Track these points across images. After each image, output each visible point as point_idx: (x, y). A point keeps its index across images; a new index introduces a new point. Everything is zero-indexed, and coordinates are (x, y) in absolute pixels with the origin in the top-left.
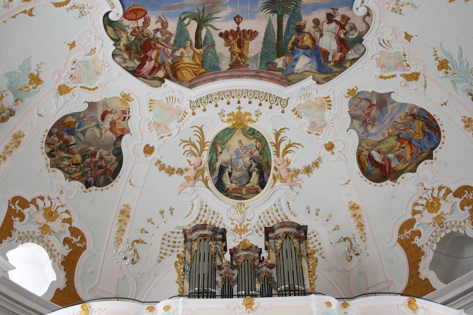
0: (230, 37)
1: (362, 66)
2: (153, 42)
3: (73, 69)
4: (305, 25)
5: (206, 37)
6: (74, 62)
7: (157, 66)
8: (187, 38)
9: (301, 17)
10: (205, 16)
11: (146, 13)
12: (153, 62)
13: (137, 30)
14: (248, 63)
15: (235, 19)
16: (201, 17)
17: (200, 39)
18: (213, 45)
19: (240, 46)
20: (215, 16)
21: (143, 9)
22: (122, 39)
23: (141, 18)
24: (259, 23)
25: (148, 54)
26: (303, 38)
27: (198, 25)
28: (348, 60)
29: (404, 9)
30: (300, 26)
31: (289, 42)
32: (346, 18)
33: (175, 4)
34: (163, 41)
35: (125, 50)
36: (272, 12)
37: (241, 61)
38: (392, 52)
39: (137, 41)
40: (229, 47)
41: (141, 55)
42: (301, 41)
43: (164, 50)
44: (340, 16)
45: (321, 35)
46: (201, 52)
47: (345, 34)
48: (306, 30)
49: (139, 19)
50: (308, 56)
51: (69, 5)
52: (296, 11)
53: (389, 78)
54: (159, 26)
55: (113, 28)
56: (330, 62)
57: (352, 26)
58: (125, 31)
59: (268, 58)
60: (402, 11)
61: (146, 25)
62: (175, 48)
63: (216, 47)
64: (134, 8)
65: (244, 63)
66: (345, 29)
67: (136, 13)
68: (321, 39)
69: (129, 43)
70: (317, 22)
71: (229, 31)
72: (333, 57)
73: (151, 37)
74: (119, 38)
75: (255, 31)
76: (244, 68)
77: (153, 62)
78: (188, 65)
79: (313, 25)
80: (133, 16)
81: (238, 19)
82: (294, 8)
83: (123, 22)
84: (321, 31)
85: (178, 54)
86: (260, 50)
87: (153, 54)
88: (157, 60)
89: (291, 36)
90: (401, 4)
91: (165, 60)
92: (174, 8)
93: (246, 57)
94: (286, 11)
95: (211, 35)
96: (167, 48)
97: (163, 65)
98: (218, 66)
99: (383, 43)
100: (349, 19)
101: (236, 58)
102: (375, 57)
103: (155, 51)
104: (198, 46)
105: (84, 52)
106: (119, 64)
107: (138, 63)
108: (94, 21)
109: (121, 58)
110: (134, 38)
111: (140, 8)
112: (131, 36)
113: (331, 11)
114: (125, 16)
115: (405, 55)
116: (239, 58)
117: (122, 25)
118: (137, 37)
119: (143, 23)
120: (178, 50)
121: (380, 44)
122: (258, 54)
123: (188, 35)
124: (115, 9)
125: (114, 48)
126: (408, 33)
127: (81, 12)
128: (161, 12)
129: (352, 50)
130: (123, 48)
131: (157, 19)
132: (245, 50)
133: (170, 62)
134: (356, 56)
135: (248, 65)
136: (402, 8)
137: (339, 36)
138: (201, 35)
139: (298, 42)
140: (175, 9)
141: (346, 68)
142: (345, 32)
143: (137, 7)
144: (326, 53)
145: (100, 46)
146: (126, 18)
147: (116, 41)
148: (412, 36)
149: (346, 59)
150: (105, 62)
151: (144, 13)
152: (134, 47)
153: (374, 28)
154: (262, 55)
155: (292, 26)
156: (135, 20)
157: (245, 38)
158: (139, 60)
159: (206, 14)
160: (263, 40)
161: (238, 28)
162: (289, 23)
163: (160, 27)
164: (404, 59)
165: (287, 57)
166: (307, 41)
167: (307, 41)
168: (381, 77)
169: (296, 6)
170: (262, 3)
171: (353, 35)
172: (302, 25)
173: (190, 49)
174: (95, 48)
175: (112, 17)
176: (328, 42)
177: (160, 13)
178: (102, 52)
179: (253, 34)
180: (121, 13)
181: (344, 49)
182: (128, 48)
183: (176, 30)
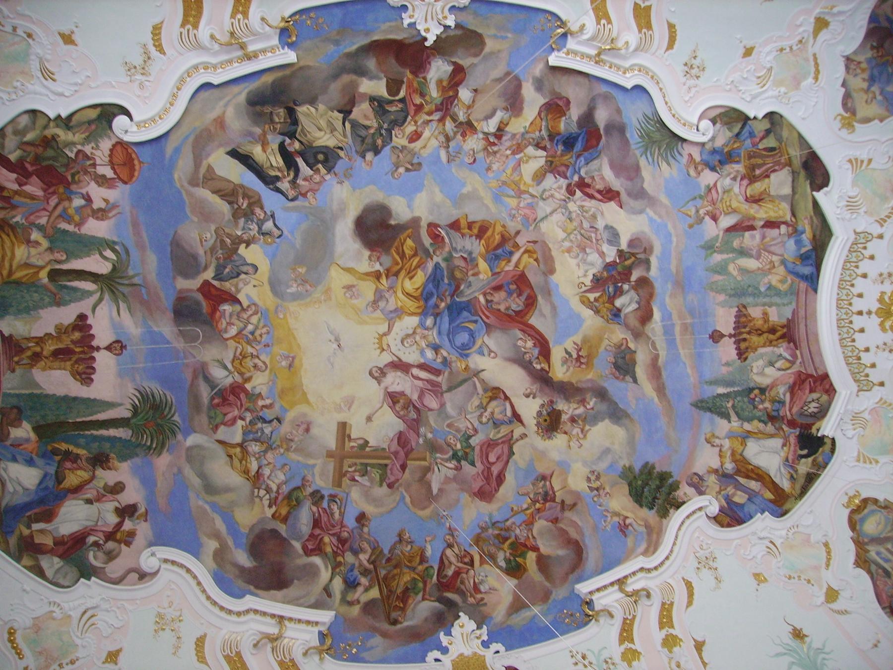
0: (77, 335)
1: (28, 589)
2: (61, 190)
3: (15, 29)
4: (110, 469)
5: (75, 289)
6: (30, 36)
7: (5, 194)
8: (71, 255)
9: (126, 460)
10: (121, 288)
11: (125, 183)
12: (16, 187)
13: (89, 163)
14: (19, 371)
15: (117, 342)
16: (117, 280)
17: (70, 278)
18: (58, 303)
19: (56, 354)
20: (121, 304)
21: (134, 179)
22: (70, 135)
23: (115, 173)
24: (111, 385)
25: (34, 179)
26: (80, 468)
27: (102, 275)
28: (37, 560)
29: (167, 636)
30: (107, 459)
31: (71, 443)
32: (130, 539)
33: (144, 235)
34: (65, 210)
35: (45, 137)
36: (135, 407)
37: (24, 356)
38: (75, 638)
39: (65, 161)
40: (54, 333)
41: (32, 165)
42: (75, 465)
43: (45, 209)
44: (132, 527)
45: (89, 502)
46: (40, 279)
47: (96, 544)
48: (99, 472)
49: (113, 168)
50: (41, 483)
51: (152, 49)
52: (138, 450)
53: (14, 648)
54: (98, 204)
55: (95, 120)
56: (29, 527)
57: (114, 553)
58: (87, 140)
59: (31, 409)
60: (161, 633)
61: (100, 181)
62: (50, 231)
63: (55, 308)
64: (136, 162)
65: (17, 363)
66: (106, 542)
67: (124, 164)
68: (81, 502)
69: (60, 146)
70: (118, 488)
71: (91, 332)
72: (41, 531)
73: (74, 187)
74: (72, 127)
75: (92, 380)
76: (6, 365)
77: (16, 187)
78: (9, 254)
79: (111, 483)
80: (119, 157)
81: (117, 347)
82: (145, 444)
83: (106, 140)
84: (99, 499)
85: (35, 235)
86: (51, 393)
87: (34, 188)
88: (20, 195)
89: (86, 447)
90: (176, 626)
91: (19, 210)
92: (137, 233)
93: (32, 366)
94: (138, 431)
95: (80, 300)
96: (50, 217)
97: (6, 205)
98: (8, 314)
99: (88, 615)
100: (128, 544)
101: (29, 348)
102: (52, 608)
103: (40, 193)
104: (54, 275)
105: (49, 57)
106: (12, 121)
107: (13, 157)
108: (114, 87)
109: (26, 126)
110: (72, 156)
111: (136, 174)
112: (75, 150)
113: (142, 510)
114: (120, 144)
115: (72, 662)
116: (29, 353)
117: (101, 137)
118: (74, 161)
119: (104, 176)
120: (45, 237)
121: (85, 612)
122: (41, 388)
123: (78, 257)
124: (135, 129)
125: (52, 115)
126: (121, 655)
127: (135, 67)
128: (128, 209)
129: (62, 563)
130: (49, 132)
131: (112, 201)
132: (49, 364)
133: (15, 220)
134: (49, 573)
135: (13, 371)
136: (168, 631)
137: (89, 534)
138: (80, 280)
139: (71, 460)
140: (134, 234)
141: (18, 560)
142: (101, 542)
143: (137, 167)
144: (48, 516)
145: (60, 90)
146: (114, 146)
147: (66, 122)
148: (116, 664)
149: (40, 557)
150: (22, 94)
151: (125, 179)
152: (50, 153)
153: (120, 592)
154: (38, 396)
155: (108, 445)
156: (110, 161)
157: (76, 362)
158: (21, 161)
159: (125, 290)
160: (73, 395)
161: (98, 349)
162: (112, 440)
163: (95, 206)
164: (64, 662)
165: (36, 445)
166: (72, 479)
167: (72, 479)
168: (11, 633)
169: (150, 448)
170: (153, 388)
171: (94, 558)
172: (110, 464)
173: (47, 259)
174: (54, 80)
175: (120, 121)
176: (73, 517)
177: (126, 206)
178: (44, 91)
179: (86, 376)
180: (127, 138)
181: (61, 549)
182: (48, 142)
183: (89, 233)
